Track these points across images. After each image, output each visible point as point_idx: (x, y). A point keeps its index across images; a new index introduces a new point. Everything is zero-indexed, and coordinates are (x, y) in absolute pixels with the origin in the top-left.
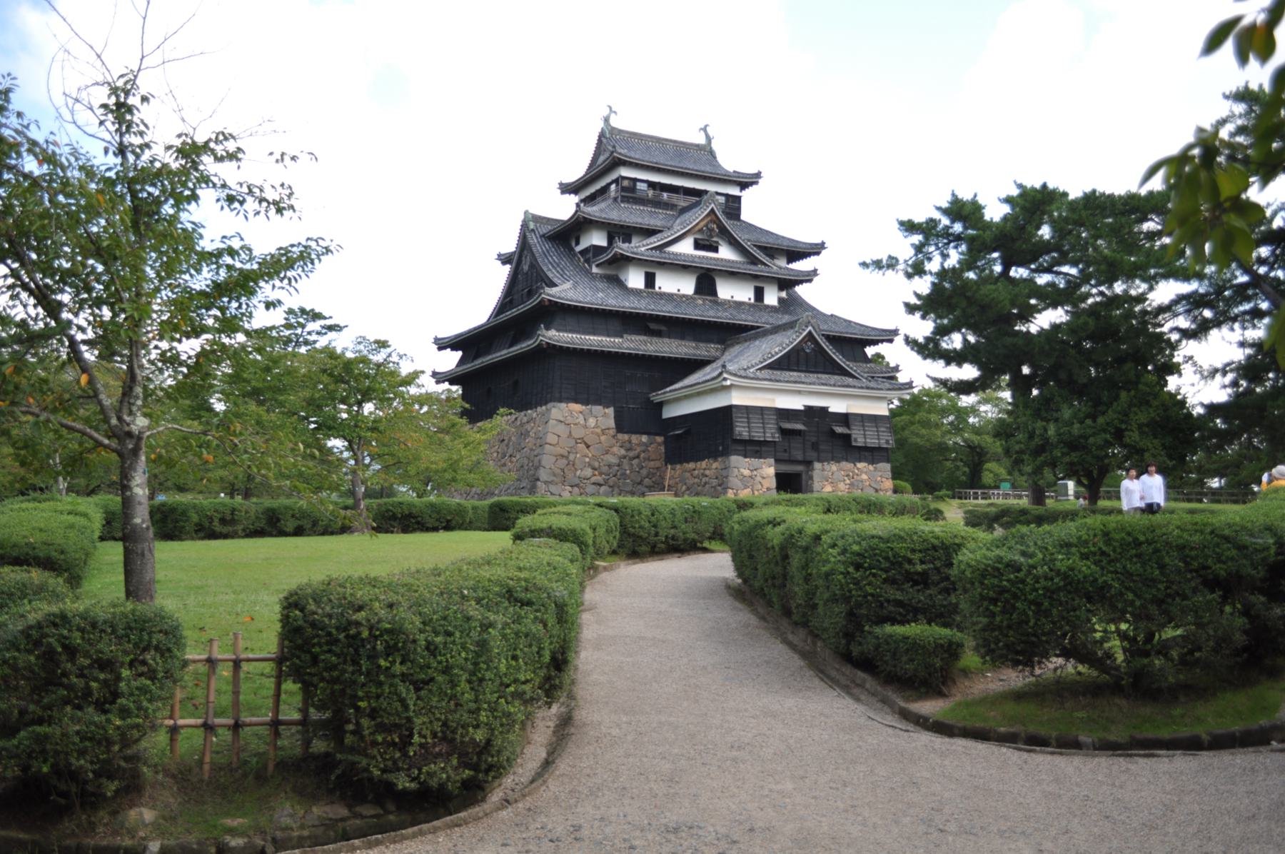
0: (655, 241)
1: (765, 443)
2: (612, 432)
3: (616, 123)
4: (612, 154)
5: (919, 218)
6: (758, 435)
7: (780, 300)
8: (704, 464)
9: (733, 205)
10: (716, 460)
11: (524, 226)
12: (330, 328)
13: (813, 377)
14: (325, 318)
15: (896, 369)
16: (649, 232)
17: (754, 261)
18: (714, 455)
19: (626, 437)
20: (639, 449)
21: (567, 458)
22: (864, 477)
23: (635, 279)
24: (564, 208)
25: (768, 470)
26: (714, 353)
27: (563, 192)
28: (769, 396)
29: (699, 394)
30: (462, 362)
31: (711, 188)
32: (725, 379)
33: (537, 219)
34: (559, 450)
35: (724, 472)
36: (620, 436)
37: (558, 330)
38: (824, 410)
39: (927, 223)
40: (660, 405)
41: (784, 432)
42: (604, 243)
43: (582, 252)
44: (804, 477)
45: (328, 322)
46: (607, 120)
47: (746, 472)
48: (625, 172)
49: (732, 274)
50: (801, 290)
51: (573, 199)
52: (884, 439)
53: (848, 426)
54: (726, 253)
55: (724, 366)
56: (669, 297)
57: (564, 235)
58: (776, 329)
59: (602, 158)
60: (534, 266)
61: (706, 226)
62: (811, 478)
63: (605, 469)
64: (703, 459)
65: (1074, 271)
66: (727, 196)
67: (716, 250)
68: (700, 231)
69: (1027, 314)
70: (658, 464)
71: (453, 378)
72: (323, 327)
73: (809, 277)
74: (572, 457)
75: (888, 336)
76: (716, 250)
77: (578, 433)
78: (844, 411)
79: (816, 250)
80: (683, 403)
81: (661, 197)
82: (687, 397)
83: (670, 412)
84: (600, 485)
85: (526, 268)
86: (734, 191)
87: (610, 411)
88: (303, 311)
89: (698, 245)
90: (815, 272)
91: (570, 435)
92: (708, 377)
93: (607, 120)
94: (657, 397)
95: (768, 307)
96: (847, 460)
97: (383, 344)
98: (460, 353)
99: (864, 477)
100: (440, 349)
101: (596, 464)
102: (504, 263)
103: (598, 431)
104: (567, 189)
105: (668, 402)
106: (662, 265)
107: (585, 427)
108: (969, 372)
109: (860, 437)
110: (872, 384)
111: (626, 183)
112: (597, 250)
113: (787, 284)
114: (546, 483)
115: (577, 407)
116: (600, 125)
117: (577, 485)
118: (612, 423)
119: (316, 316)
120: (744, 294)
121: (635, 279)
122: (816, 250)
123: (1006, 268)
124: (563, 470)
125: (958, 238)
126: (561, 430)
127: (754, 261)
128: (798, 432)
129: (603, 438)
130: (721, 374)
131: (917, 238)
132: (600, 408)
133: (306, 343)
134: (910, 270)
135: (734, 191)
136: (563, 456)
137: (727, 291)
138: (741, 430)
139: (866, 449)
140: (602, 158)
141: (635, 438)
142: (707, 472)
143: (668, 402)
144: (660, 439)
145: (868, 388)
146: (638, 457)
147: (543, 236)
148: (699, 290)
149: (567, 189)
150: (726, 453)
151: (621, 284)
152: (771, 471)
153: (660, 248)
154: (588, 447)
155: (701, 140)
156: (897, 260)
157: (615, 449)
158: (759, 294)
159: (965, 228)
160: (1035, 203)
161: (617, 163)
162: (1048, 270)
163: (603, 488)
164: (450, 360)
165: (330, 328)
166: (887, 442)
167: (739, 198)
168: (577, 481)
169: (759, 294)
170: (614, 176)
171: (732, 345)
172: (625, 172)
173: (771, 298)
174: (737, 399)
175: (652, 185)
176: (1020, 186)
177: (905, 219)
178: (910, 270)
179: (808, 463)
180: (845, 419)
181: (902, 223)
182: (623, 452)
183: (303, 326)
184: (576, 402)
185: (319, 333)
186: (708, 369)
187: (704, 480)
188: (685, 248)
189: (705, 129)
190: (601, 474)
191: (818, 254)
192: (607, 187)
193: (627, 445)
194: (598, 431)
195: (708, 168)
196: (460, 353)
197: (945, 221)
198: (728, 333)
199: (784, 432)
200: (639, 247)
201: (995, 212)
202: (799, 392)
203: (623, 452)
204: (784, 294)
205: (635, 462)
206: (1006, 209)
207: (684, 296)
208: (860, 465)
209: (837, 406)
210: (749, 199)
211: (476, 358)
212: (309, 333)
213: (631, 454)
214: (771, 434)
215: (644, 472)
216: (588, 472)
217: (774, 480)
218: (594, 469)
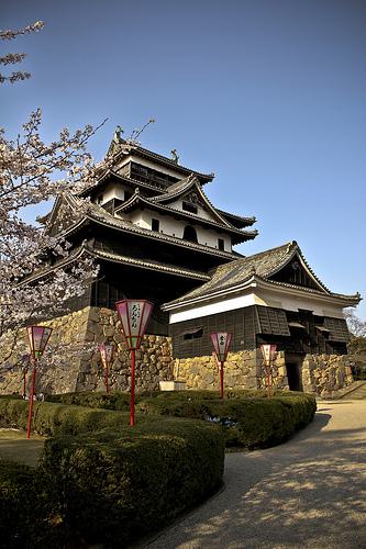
41: (292, 329)
49: (206, 227)
73: (251, 237)
79: (250, 223)
83: (174, 319)
89: (185, 207)
112: (117, 202)
122: (250, 223)
146: (154, 353)
155: (171, 157)
175: (150, 170)
202: (295, 298)
209: (318, 312)
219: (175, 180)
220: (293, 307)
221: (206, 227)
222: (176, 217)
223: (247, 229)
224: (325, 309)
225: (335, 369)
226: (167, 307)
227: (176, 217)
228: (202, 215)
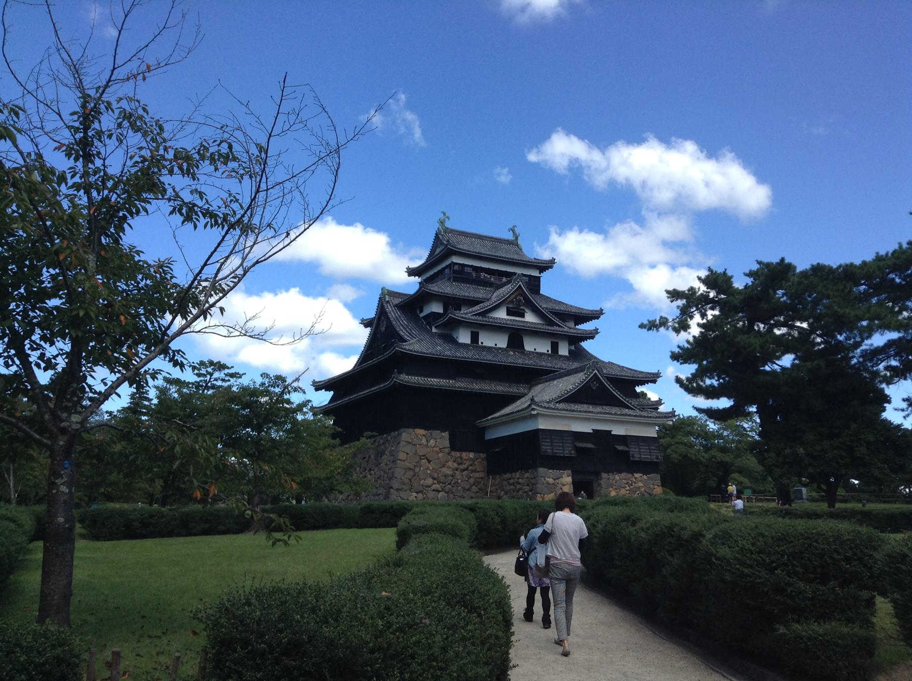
2: (447, 450)
3: (449, 225)
5: (683, 287)
6: (558, 452)
7: (570, 351)
8: (518, 475)
9: (534, 284)
10: (527, 472)
12: (232, 375)
13: (599, 409)
14: (228, 368)
15: (659, 402)
16: (473, 302)
17: (551, 323)
18: (525, 467)
19: (458, 454)
20: (467, 463)
21: (413, 470)
22: (641, 484)
23: (464, 337)
24: (410, 285)
26: (522, 390)
27: (409, 275)
28: (566, 422)
29: (513, 421)
30: (332, 401)
31: (519, 271)
32: (533, 409)
34: (407, 464)
35: (533, 481)
36: (453, 453)
37: (407, 375)
39: (689, 290)
40: (483, 430)
41: (578, 450)
42: (441, 311)
43: (424, 317)
44: (595, 485)
45: (231, 371)
47: (551, 481)
48: (456, 260)
49: (535, 333)
50: (586, 345)
51: (417, 279)
52: (653, 455)
53: (627, 446)
54: (530, 318)
55: (532, 400)
56: (489, 349)
57: (411, 305)
58: (569, 373)
59: (438, 250)
60: (390, 327)
61: (515, 298)
62: (600, 485)
63: (442, 479)
64: (516, 471)
65: (805, 325)
68: (512, 302)
69: (772, 357)
70: (482, 475)
71: (326, 411)
72: (226, 375)
73: (591, 335)
74: (417, 470)
75: (652, 378)
77: (422, 451)
79: (596, 315)
80: (504, 426)
82: (504, 423)
84: (439, 491)
85: (383, 329)
86: (535, 273)
87: (446, 435)
88: (211, 363)
89: (509, 313)
90: (596, 331)
91: (416, 454)
92: (520, 408)
93: (442, 223)
95: (561, 356)
98: (332, 393)
99: (641, 484)
100: (317, 389)
101: (436, 475)
102: (366, 326)
103: (437, 449)
104: (411, 272)
105: (489, 427)
107: (427, 446)
108: (724, 403)
109: (637, 454)
110: (644, 414)
111: (456, 267)
113: (575, 340)
114: (397, 490)
115: (421, 432)
116: (436, 226)
117: (421, 492)
119: (221, 366)
120: (543, 347)
121: (464, 337)
122: (596, 315)
123: (751, 324)
124: (410, 480)
125: (714, 303)
126: (409, 449)
127: (551, 323)
128: (590, 449)
129: (440, 455)
130: (530, 405)
131: (681, 302)
132: (438, 432)
133: (213, 387)
134: (677, 325)
135: (535, 273)
136: (410, 469)
137: (530, 345)
138: (546, 448)
140: (438, 250)
141: (464, 455)
142: (521, 481)
143: (489, 427)
144: (483, 455)
145: (641, 416)
146: (467, 469)
147: (396, 306)
148: (510, 345)
149: (411, 272)
150: (535, 467)
151: (454, 342)
152: (570, 479)
153: (484, 314)
154: (429, 462)
155: (510, 236)
156: (667, 320)
157: (450, 464)
158: (555, 348)
159: (718, 293)
160: (774, 274)
161: (450, 252)
162: (784, 325)
163: (441, 494)
164: (324, 398)
165: (232, 375)
166: (657, 458)
168: (421, 489)
169: (555, 348)
170: (448, 262)
171: (536, 385)
172: (456, 260)
173: (564, 350)
174: (543, 425)
175: (476, 269)
176: (759, 263)
177: (671, 289)
178: (677, 325)
179: (597, 474)
180: (624, 439)
181: (668, 292)
182: (455, 465)
183: (211, 375)
185: (223, 380)
186: (519, 402)
187: (518, 486)
188: (501, 314)
189: (513, 230)
190: (439, 483)
191: (598, 318)
192: (444, 269)
193: (459, 460)
194: (437, 449)
195: (516, 257)
196: (332, 393)
197: (703, 288)
198: (533, 375)
199: (578, 450)
200: (466, 313)
201: (740, 283)
202: (589, 419)
204: (573, 348)
205: (466, 472)
206: (749, 281)
207: (500, 349)
208: (636, 475)
209: (618, 430)
211: (345, 395)
212: (216, 380)
213: (462, 467)
214: (568, 451)
215: (472, 480)
216: (429, 481)
218: (434, 479)
220: (586, 428)
222: (497, 328)
224: (628, 427)
227: (497, 328)
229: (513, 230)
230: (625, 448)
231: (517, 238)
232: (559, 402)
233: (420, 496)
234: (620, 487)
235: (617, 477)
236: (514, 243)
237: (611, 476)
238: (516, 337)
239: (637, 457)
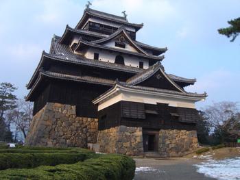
0: (98, 41)
1: (137, 119)
3: (90, 7)
4: (88, 14)
6: (134, 115)
9: (133, 36)
11: (53, 40)
19: (81, 118)
25: (139, 132)
33: (57, 37)
38: (167, 105)
40: (98, 104)
41: (147, 115)
46: (88, 6)
48: (90, 20)
49: (130, 56)
53: (177, 113)
66: (131, 32)
67: (124, 47)
70: (95, 130)
76: (124, 47)
78: (176, 106)
81: (106, 30)
83: (100, 108)
87: (74, 108)
89: (116, 45)
91: (54, 117)
93: (88, 6)
94: (95, 102)
96: (177, 129)
97: (9, 85)
99: (185, 137)
106: (101, 50)
111: (91, 24)
112: (75, 44)
115: (59, 105)
116: (85, 8)
117: (55, 139)
118: (74, 112)
120: (135, 65)
135: (134, 31)
137: (127, 63)
139: (185, 124)
141: (85, 119)
144: (96, 120)
146: (86, 127)
148: (116, 62)
152: (141, 133)
155: (122, 15)
158: (141, 65)
167: (135, 33)
168: (56, 137)
169: (141, 65)
172: (90, 20)
173: (146, 67)
175: (101, 25)
179: (159, 130)
184: (59, 103)
193: (81, 122)
200: (93, 43)
202: (154, 97)
203: (78, 125)
205: (84, 129)
208: (182, 131)
209: (173, 104)
210: (137, 33)
213: (83, 126)
214: (141, 115)
215: (88, 134)
217: (142, 138)
219: (116, 29)
220: (153, 102)
221: (130, 56)
222: (110, 52)
223: (161, 55)
225: (184, 139)
226: (95, 102)
227: (110, 52)
228: (129, 49)
229: (124, 12)
230: (176, 115)
231: (126, 17)
232: (136, 85)
233: (55, 141)
234: (173, 139)
235: (171, 132)
236: (125, 18)
237: (167, 131)
238: (120, 58)
239: (183, 120)
